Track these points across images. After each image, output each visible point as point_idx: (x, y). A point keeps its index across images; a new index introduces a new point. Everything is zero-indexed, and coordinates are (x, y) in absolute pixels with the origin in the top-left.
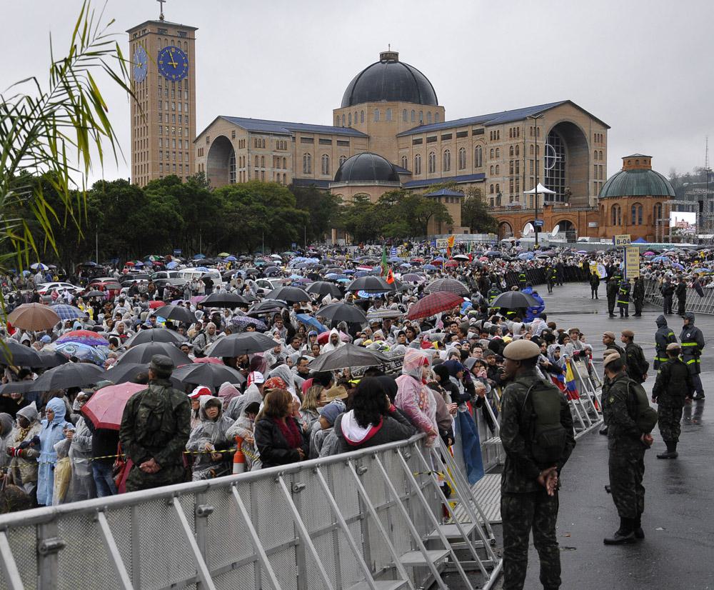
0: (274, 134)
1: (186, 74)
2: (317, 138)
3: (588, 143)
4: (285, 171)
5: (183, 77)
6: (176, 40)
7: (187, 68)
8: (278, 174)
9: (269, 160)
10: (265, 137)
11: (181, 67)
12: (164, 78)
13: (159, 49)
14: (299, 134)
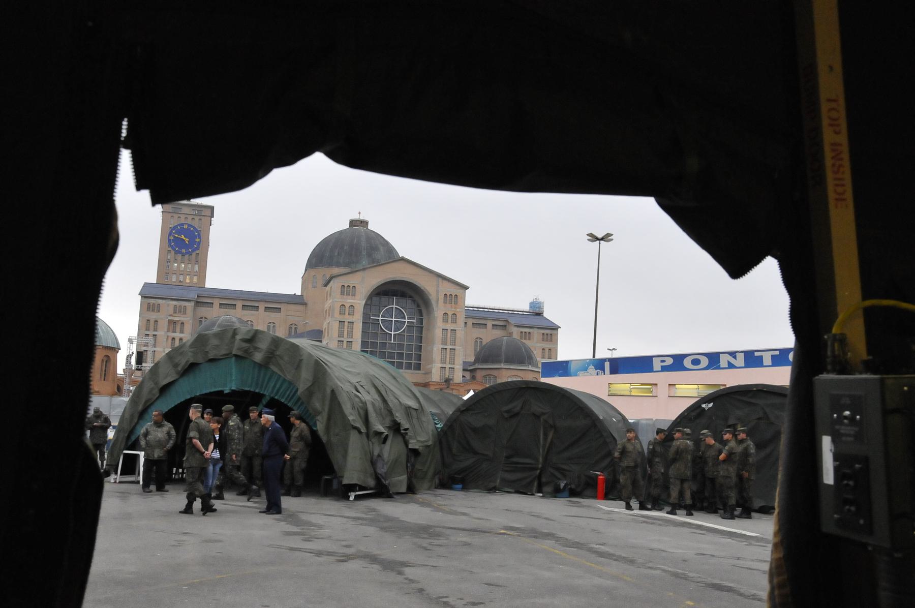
0: (172, 299)
1: (198, 248)
2: (239, 304)
3: (433, 302)
4: (182, 335)
5: (193, 251)
6: (190, 217)
7: (199, 243)
8: (173, 339)
9: (163, 324)
10: (160, 301)
11: (192, 241)
12: (173, 252)
13: (172, 226)
14: (241, 301)
